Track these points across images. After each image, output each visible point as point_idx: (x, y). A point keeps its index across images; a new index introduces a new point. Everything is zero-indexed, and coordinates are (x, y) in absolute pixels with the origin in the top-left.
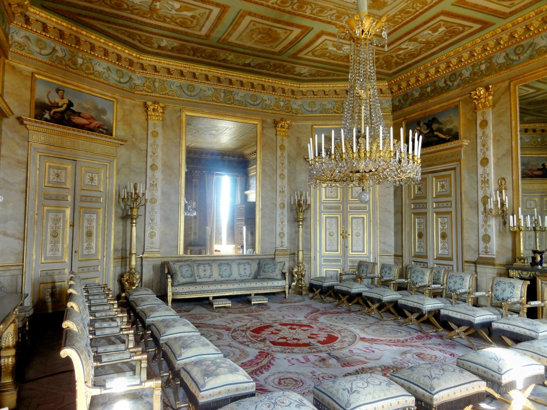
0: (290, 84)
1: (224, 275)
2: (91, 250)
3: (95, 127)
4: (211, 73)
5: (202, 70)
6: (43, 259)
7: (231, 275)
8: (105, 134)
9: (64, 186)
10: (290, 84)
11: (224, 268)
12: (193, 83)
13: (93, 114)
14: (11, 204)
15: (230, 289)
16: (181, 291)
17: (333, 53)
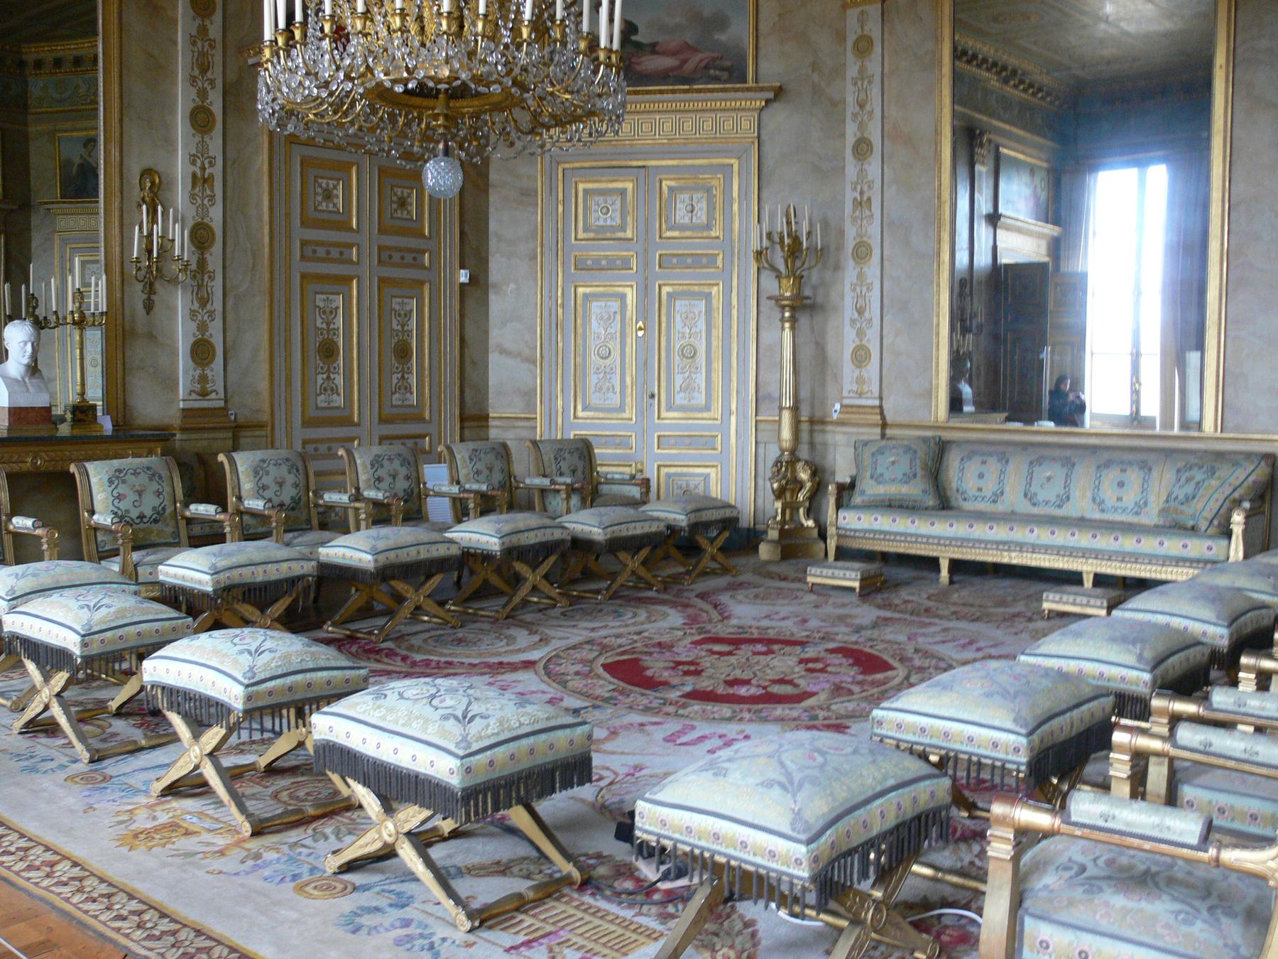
1: (1040, 497)
2: (696, 394)
3: (695, 70)
6: (579, 407)
7: (1064, 499)
8: (725, 82)
9: (621, 235)
11: (1043, 472)
13: (690, 37)
14: (512, 286)
15: (998, 543)
16: (853, 527)
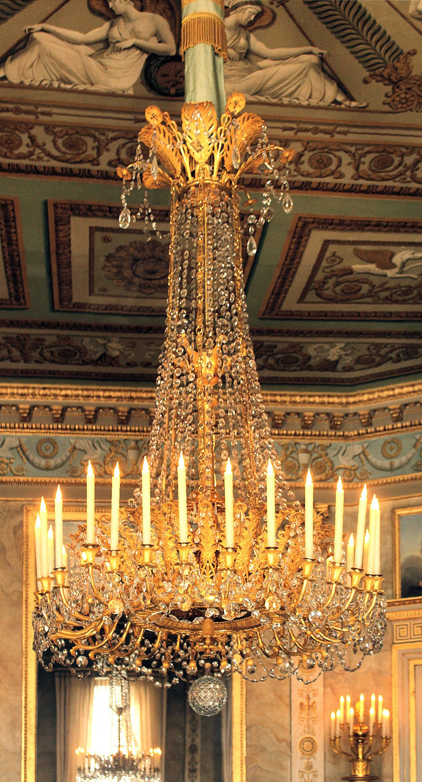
0: (317, 399)
4: (93, 401)
5: (66, 396)
10: (317, 399)
12: (52, 435)
17: (377, 281)
